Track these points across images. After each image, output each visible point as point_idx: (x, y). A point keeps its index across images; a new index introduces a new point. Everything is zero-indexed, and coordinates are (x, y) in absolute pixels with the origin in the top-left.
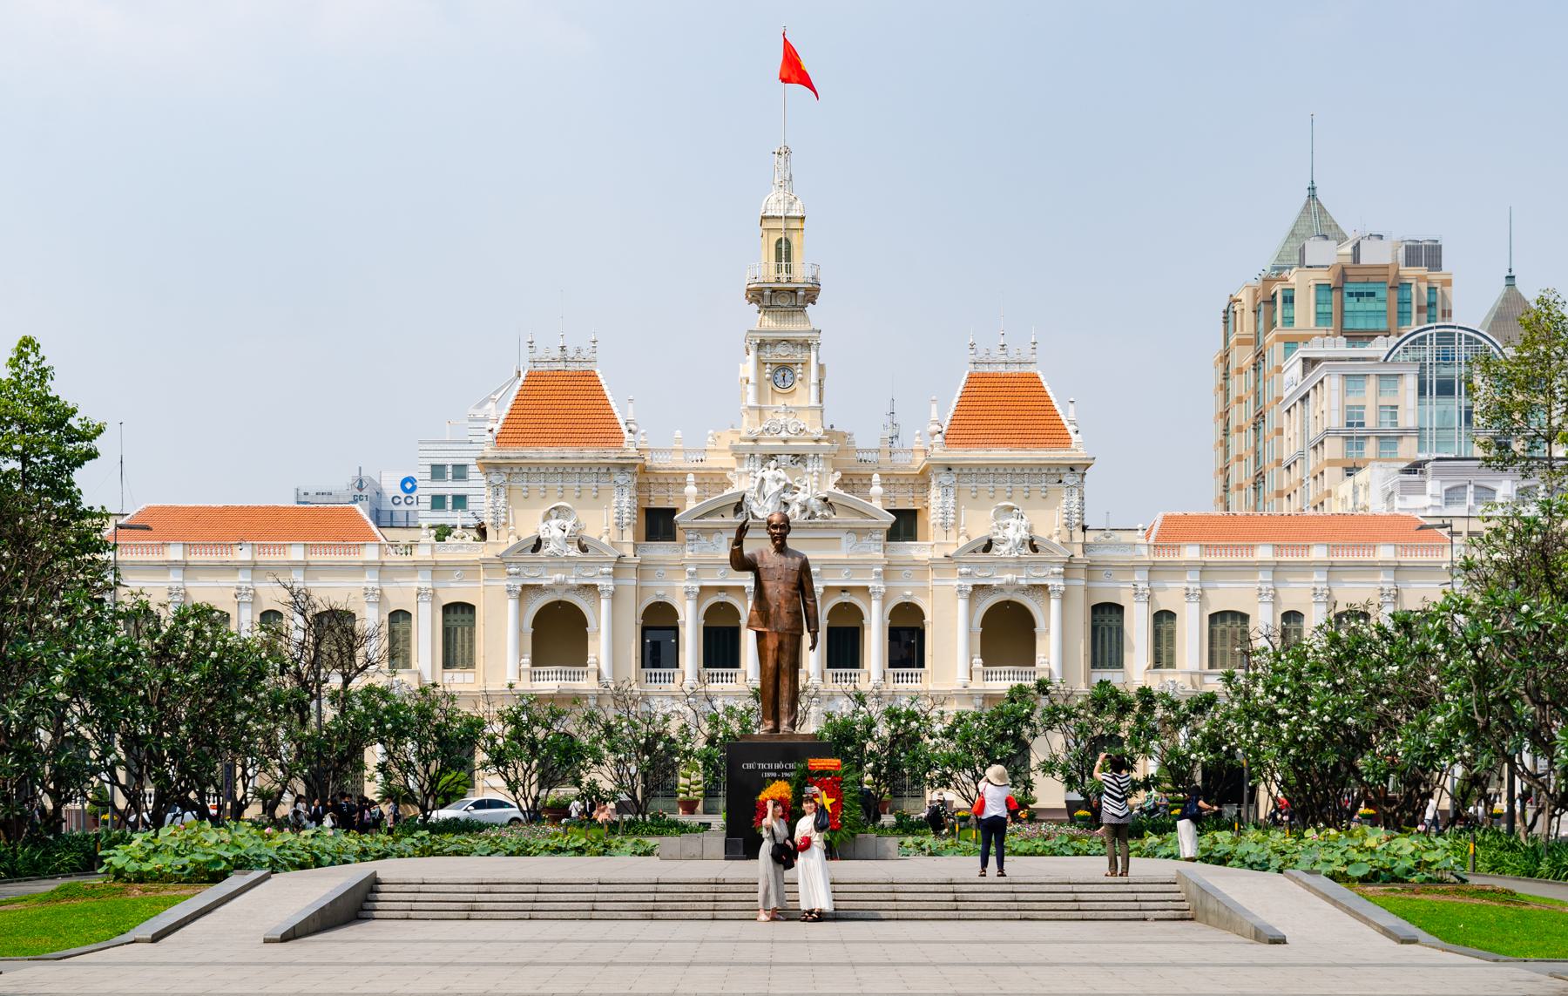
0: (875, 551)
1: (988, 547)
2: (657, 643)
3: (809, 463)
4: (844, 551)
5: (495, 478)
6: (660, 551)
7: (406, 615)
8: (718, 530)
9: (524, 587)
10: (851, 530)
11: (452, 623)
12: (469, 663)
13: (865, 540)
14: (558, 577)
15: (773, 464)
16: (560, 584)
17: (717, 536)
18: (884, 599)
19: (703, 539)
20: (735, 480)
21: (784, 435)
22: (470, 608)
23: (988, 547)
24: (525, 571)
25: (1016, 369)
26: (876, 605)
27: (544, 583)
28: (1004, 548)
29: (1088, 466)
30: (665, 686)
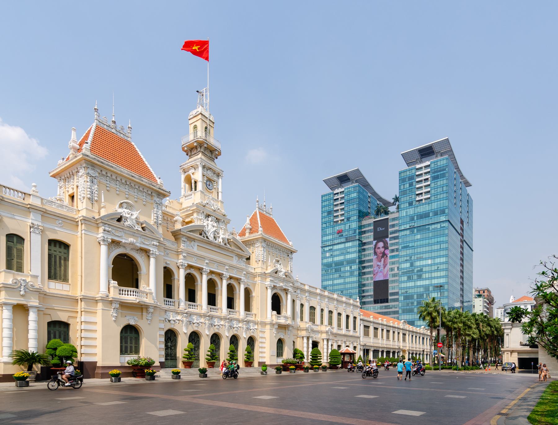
1: (276, 273)
3: (220, 223)
7: (21, 240)
8: (194, 240)
9: (113, 242)
11: (52, 252)
12: (65, 279)
14: (131, 240)
15: (210, 219)
16: (131, 244)
19: (188, 243)
20: (196, 220)
21: (213, 208)
22: (67, 246)
24: (113, 231)
25: (268, 215)
27: (123, 241)
29: (295, 252)
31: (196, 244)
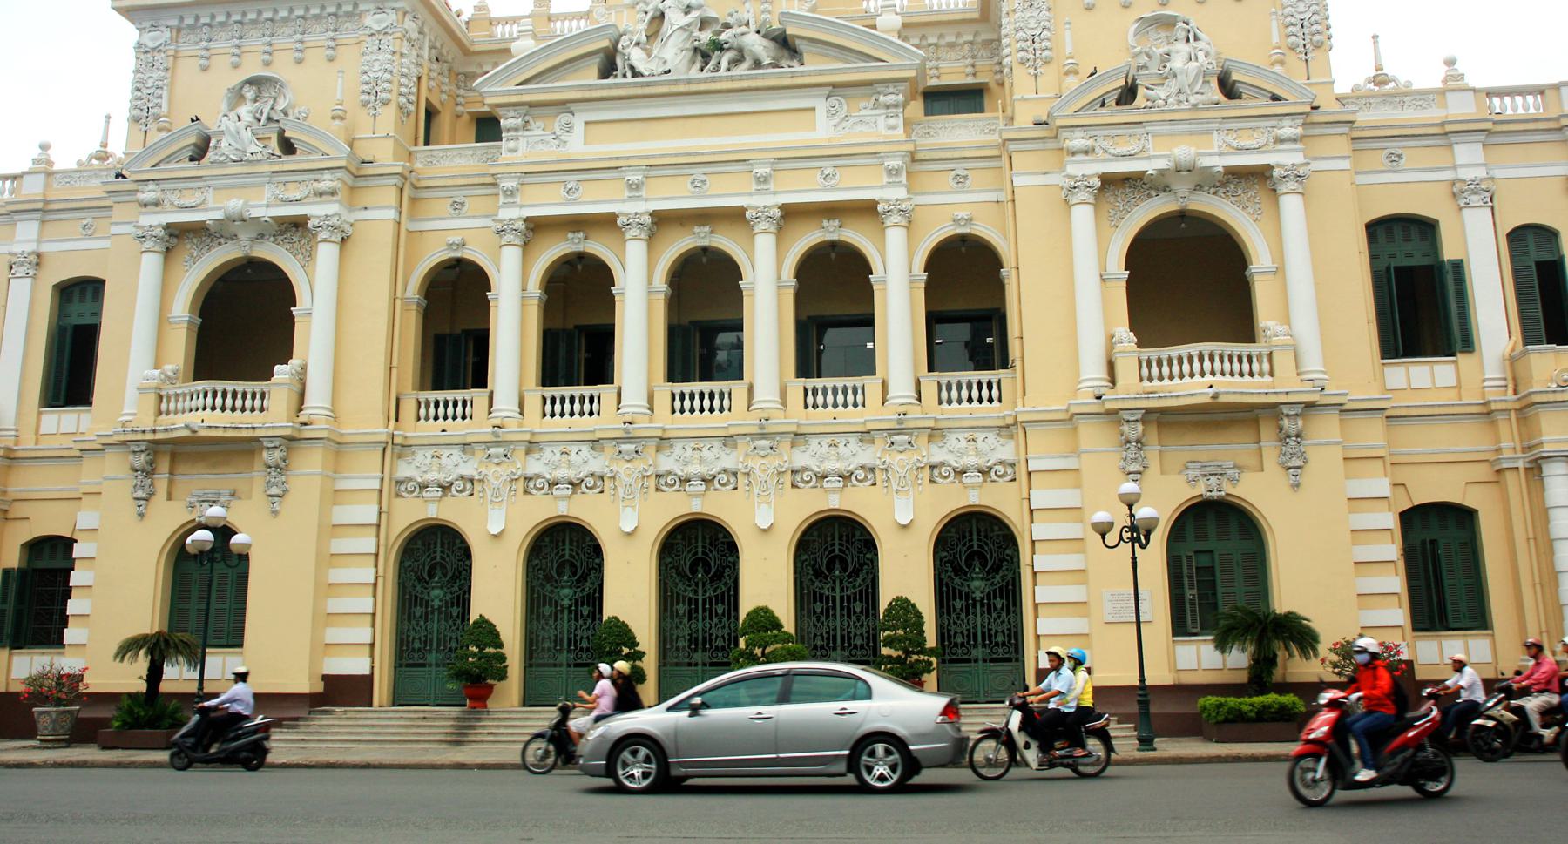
0: (882, 126)
1: (1128, 94)
2: (451, 343)
4: (823, 126)
5: (150, 40)
6: (457, 158)
8: (562, 105)
10: (836, 88)
13: (863, 109)
17: (565, 118)
18: (909, 225)
19: (537, 129)
23: (1128, 94)
26: (895, 238)
28: (1161, 93)
30: (457, 429)
31: (578, 122)
